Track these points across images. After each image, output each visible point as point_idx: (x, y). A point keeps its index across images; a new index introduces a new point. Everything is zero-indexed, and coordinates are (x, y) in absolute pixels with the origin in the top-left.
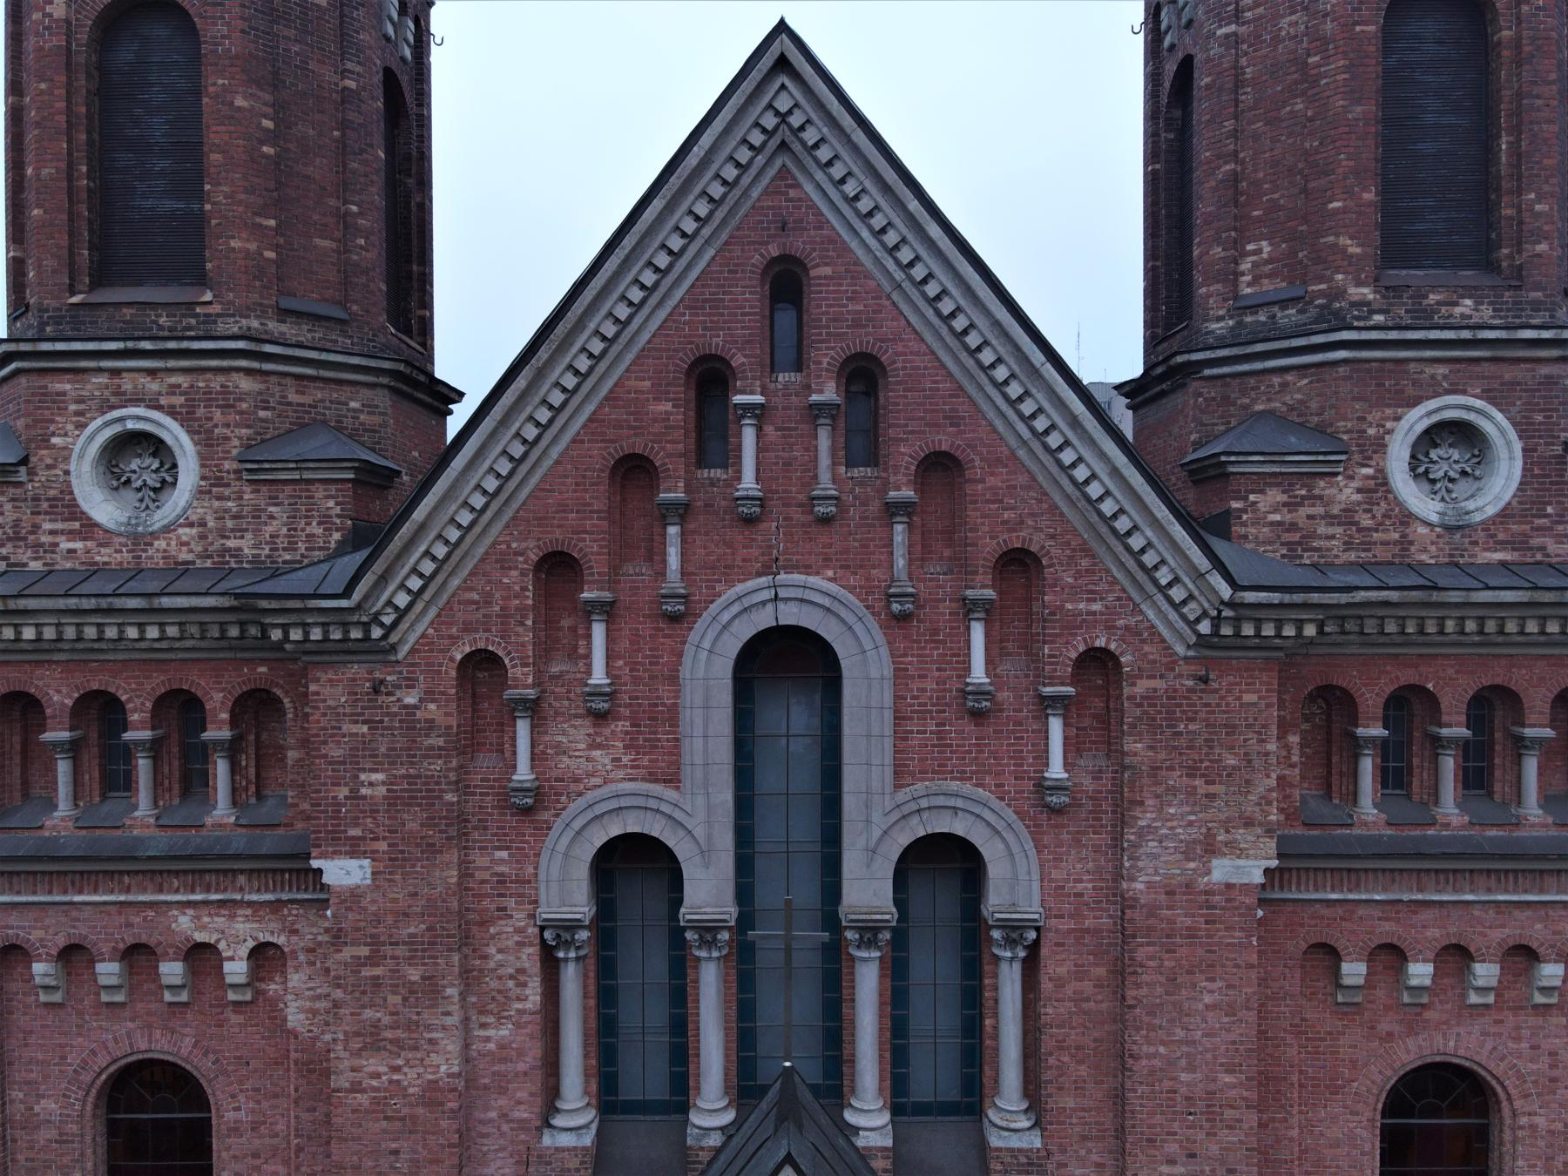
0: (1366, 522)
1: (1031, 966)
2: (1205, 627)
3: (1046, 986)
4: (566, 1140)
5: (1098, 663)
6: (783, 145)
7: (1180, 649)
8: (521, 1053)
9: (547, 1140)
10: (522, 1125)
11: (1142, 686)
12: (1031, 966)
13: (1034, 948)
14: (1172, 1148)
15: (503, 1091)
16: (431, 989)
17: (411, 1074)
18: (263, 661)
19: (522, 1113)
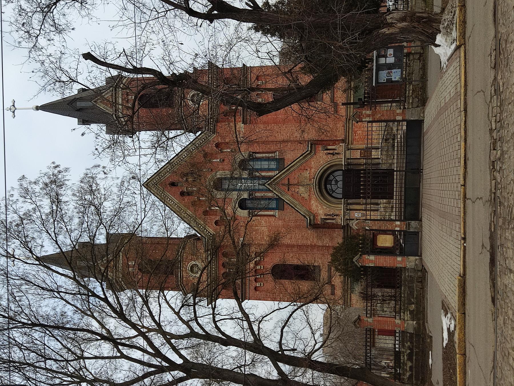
0: (203, 109)
1: (256, 153)
2: (211, 133)
3: (257, 151)
4: (277, 214)
5: (217, 145)
6: (156, 185)
7: (215, 135)
8: (266, 220)
9: (277, 216)
10: (275, 220)
11: (220, 140)
12: (256, 153)
13: (253, 153)
14: (277, 135)
15: (271, 222)
16: (256, 230)
17: (267, 233)
18: (219, 254)
19: (273, 220)
